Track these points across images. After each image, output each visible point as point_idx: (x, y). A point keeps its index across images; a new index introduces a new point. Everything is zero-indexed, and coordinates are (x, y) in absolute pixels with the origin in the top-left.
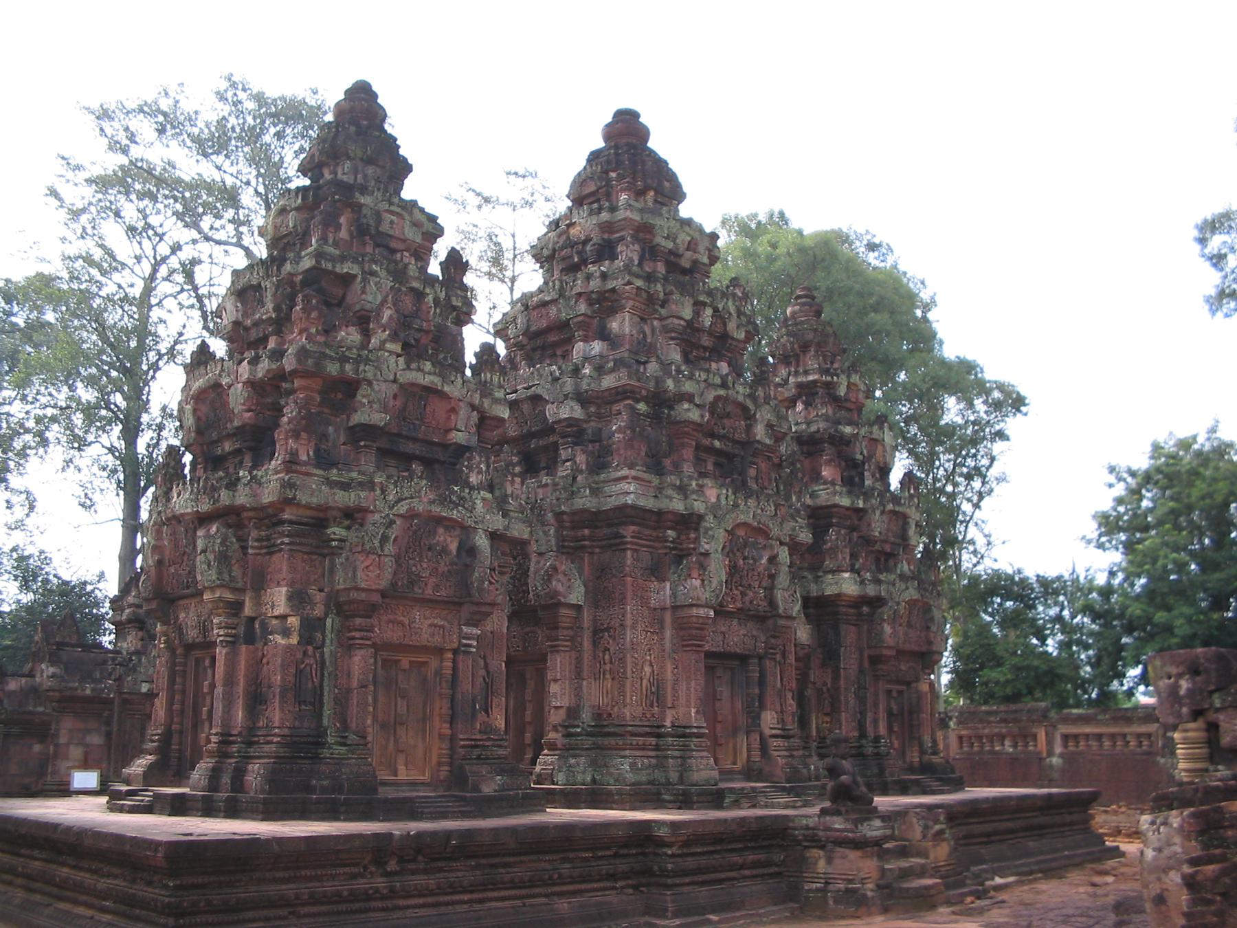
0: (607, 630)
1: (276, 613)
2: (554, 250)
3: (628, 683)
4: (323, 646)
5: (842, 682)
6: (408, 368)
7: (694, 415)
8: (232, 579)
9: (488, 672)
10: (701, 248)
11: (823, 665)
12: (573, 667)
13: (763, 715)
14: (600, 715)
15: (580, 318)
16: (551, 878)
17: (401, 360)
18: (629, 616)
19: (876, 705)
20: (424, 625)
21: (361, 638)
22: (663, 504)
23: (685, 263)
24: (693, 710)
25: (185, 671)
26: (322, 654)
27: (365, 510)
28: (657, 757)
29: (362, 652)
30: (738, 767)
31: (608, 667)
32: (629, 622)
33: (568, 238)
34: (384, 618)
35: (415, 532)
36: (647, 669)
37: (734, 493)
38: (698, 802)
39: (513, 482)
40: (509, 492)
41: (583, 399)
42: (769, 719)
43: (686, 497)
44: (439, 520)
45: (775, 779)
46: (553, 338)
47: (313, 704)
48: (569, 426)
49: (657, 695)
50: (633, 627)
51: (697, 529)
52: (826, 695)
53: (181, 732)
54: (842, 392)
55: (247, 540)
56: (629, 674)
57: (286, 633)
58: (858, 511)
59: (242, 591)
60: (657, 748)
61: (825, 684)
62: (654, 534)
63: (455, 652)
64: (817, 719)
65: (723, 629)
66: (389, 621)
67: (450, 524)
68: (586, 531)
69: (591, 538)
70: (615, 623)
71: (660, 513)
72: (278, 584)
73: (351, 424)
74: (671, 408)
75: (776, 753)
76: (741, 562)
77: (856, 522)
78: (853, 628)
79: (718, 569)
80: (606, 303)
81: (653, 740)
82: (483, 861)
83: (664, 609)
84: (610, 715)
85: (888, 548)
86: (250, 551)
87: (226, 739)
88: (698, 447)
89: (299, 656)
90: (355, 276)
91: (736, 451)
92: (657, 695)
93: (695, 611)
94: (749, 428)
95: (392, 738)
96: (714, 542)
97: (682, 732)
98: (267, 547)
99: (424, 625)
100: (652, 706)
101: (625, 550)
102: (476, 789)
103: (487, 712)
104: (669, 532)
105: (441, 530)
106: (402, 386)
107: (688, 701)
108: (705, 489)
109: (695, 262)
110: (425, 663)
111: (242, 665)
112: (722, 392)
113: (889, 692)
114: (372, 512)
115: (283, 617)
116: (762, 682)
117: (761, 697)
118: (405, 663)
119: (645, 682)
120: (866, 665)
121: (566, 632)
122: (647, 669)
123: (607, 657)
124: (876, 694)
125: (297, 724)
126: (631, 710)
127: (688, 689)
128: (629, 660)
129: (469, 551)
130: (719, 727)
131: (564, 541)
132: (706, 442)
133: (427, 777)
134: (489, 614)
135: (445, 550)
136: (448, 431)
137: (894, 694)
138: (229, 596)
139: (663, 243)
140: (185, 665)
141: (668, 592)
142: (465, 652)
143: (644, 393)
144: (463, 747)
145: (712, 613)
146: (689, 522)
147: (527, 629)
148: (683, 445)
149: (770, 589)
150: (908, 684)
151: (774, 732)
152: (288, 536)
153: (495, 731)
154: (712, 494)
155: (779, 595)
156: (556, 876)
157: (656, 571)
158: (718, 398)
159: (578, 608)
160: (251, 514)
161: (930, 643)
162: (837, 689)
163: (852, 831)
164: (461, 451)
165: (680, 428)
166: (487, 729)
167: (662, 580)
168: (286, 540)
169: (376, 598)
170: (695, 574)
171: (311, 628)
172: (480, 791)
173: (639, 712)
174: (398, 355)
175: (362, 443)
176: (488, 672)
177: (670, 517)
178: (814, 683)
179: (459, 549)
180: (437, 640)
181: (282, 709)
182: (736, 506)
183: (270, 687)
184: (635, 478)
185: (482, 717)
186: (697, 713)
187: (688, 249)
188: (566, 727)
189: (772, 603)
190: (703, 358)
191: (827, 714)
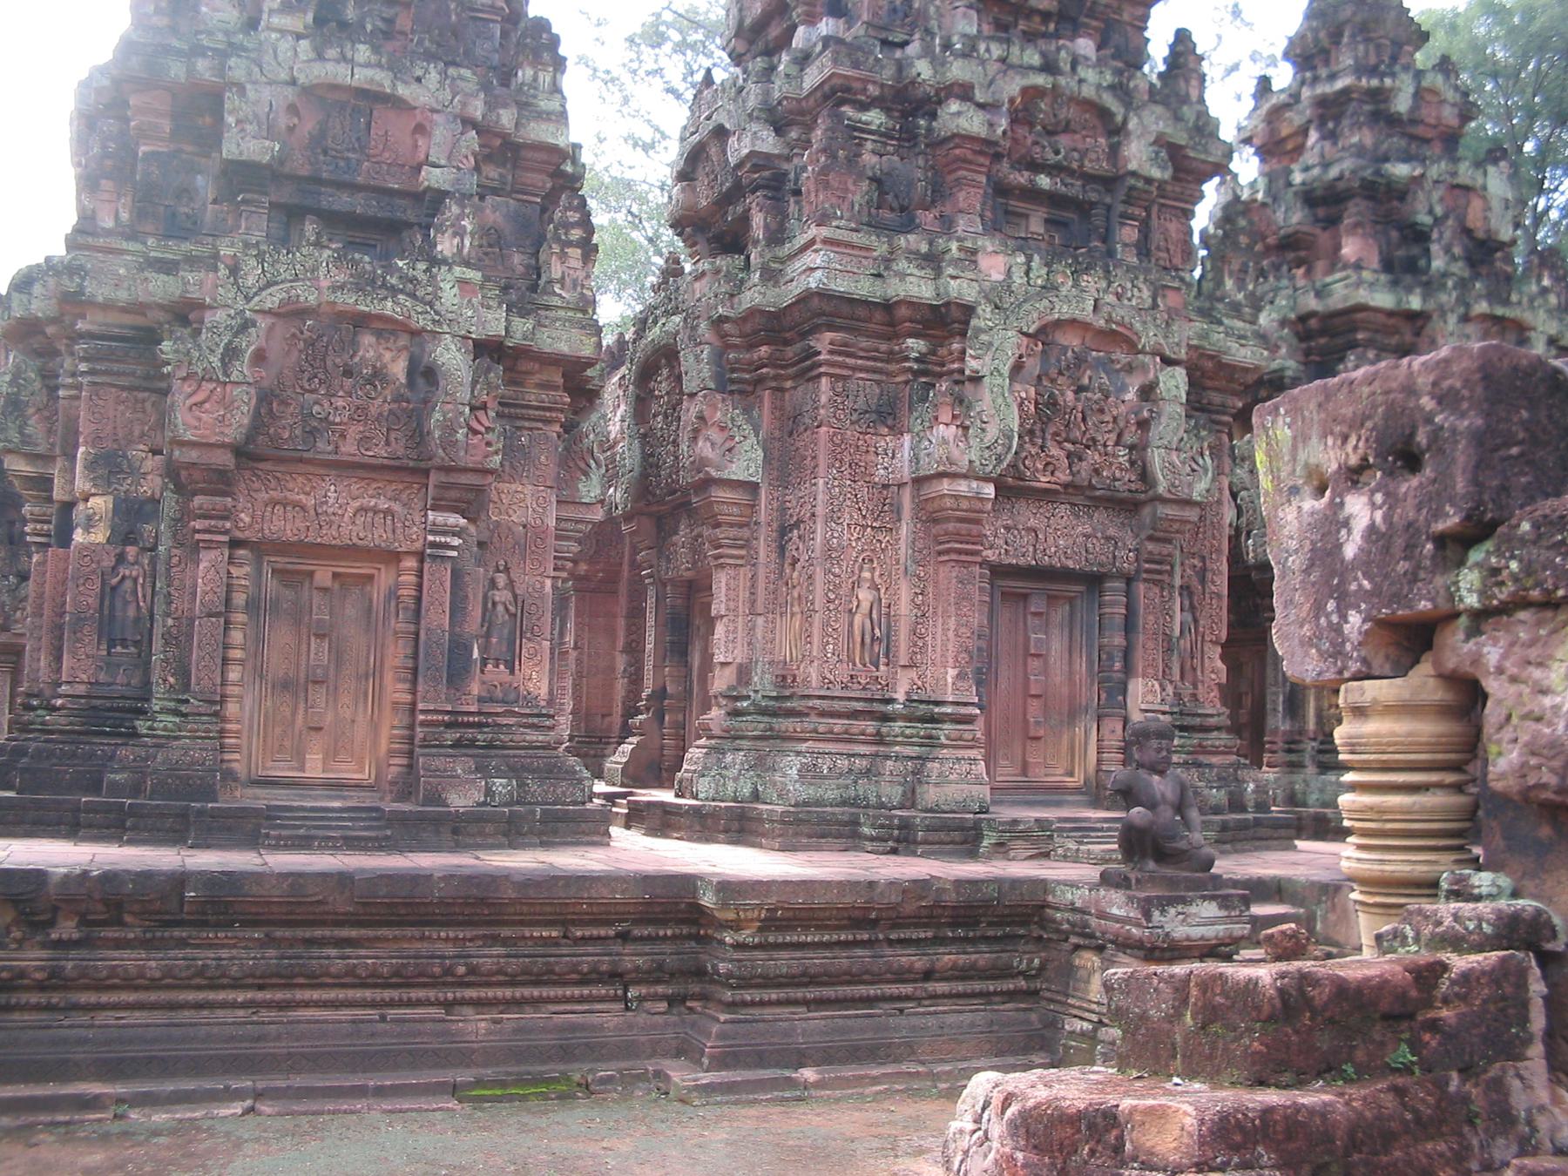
3: (817, 618)
4: (154, 548)
6: (320, 57)
7: (972, 122)
8: (26, 439)
9: (515, 596)
13: (1131, 687)
16: (449, 971)
17: (304, 44)
18: (820, 497)
20: (343, 509)
22: (896, 289)
24: (952, 673)
26: (153, 562)
27: (201, 306)
28: (876, 755)
29: (212, 554)
30: (1077, 779)
32: (820, 510)
34: (263, 496)
35: (311, 343)
36: (865, 595)
38: (926, 842)
39: (563, 257)
44: (361, 321)
47: (136, 643)
48: (756, 168)
49: (879, 643)
50: (833, 517)
51: (963, 334)
58: (1411, 316)
59: (48, 458)
62: (884, 347)
63: (421, 556)
64: (1318, 699)
65: (1032, 523)
67: (387, 328)
69: (771, 362)
70: (805, 512)
71: (888, 307)
74: (933, 116)
76: (1070, 395)
77: (1408, 338)
79: (1000, 409)
81: (870, 726)
82: (279, 933)
83: (901, 485)
88: (1001, 190)
91: (1093, 197)
92: (879, 643)
93: (945, 486)
94: (1114, 152)
95: (302, 706)
96: (993, 352)
97: (925, 713)
99: (343, 509)
102: (435, 798)
104: (910, 342)
105: (367, 339)
108: (980, 257)
110: (371, 577)
112: (1040, 80)
114: (210, 307)
116: (1129, 625)
117: (1127, 654)
118: (323, 576)
119: (858, 619)
125: (102, 677)
129: (425, 374)
130: (1034, 705)
132: (1022, 178)
135: (379, 375)
142: (434, 557)
143: (873, 90)
144: (423, 724)
146: (946, 322)
153: (530, 700)
154: (994, 265)
155: (1156, 459)
156: (461, 970)
157: (887, 416)
159: (754, 487)
163: (1138, 925)
164: (435, 200)
166: (512, 697)
167: (897, 431)
169: (225, 459)
170: (945, 416)
171: (131, 518)
174: (299, 37)
179: (411, 372)
180: (379, 536)
182: (1050, 287)
184: (826, 241)
186: (960, 676)
189: (1145, 476)
190: (1044, 35)
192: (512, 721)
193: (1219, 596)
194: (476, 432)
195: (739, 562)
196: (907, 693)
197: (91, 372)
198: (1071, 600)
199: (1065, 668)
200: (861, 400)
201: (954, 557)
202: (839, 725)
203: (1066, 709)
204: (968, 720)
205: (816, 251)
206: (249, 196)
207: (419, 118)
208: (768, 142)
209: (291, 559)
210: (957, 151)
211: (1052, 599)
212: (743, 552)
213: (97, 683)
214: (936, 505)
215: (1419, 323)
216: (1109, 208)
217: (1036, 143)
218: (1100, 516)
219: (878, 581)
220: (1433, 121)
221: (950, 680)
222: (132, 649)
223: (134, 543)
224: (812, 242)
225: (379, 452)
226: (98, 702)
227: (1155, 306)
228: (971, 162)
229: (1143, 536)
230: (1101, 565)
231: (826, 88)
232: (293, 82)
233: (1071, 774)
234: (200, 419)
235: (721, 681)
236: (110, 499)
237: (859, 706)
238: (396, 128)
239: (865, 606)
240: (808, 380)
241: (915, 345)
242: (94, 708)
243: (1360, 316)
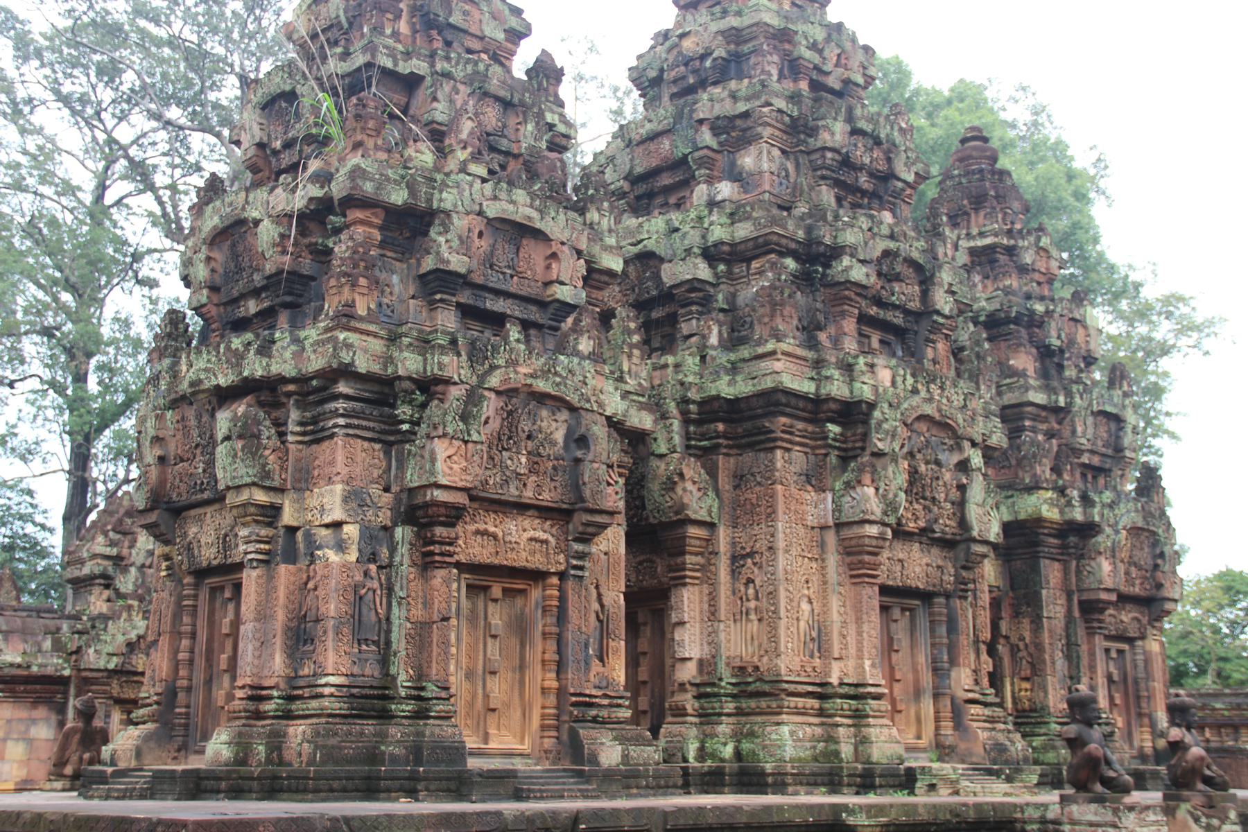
0: (751, 555)
1: (328, 519)
2: (662, 70)
3: (783, 623)
5: (1046, 634)
7: (859, 274)
9: (602, 606)
10: (854, 64)
11: (1016, 615)
12: (706, 606)
13: (953, 674)
14: (742, 669)
15: (701, 153)
18: (781, 536)
19: (1092, 668)
21: (442, 554)
23: (833, 82)
24: (867, 663)
25: (195, 606)
28: (822, 724)
30: (924, 742)
31: (752, 604)
32: (781, 544)
33: (680, 53)
34: (472, 528)
37: (913, 375)
39: (630, 356)
40: (626, 368)
41: (710, 254)
42: (962, 680)
43: (852, 380)
45: (974, 759)
46: (666, 180)
47: (376, 643)
49: (819, 642)
51: (866, 422)
52: (1023, 654)
53: (189, 689)
54: (1028, 258)
55: (285, 424)
56: (783, 613)
57: (341, 547)
58: (1056, 410)
60: (821, 713)
61: (1022, 639)
64: (1012, 684)
65: (901, 556)
66: (478, 532)
67: (559, 403)
68: (721, 427)
69: (725, 436)
70: (761, 545)
72: (330, 481)
73: (422, 271)
74: (827, 266)
75: (975, 724)
77: (1056, 426)
78: (1056, 565)
80: (736, 131)
81: (815, 703)
83: (823, 528)
84: (757, 668)
85: (1096, 461)
86: (290, 438)
87: (257, 695)
88: (863, 319)
89: (359, 577)
90: (422, 78)
92: (819, 642)
94: (925, 295)
98: (312, 432)
100: (812, 656)
101: (773, 449)
103: (602, 660)
106: (490, 221)
107: (860, 650)
108: (876, 369)
109: (847, 82)
110: (523, 591)
111: (282, 593)
112: (892, 245)
113: (1107, 651)
114: (455, 383)
115: (337, 525)
119: (802, 624)
120: (1077, 614)
121: (694, 559)
122: (805, 606)
123: (751, 591)
124: (1092, 654)
125: (356, 670)
126: (790, 662)
127: (860, 633)
128: (782, 594)
130: (897, 686)
131: (689, 439)
132: (873, 311)
133: (526, 747)
134: (604, 527)
136: (547, 284)
137: (1114, 655)
138: (261, 497)
139: (808, 54)
140: (196, 597)
141: (830, 506)
145: (889, 532)
146: (854, 414)
147: (642, 558)
148: (843, 314)
149: (961, 504)
150: (1130, 641)
151: (971, 695)
152: (342, 415)
155: (973, 512)
158: (886, 253)
159: (711, 526)
160: (291, 387)
161: (1159, 586)
162: (1039, 647)
165: (843, 291)
168: (341, 421)
169: (461, 499)
172: (598, 764)
173: (796, 664)
174: (484, 181)
175: (438, 297)
176: (602, 606)
177: (833, 406)
178: (1007, 637)
179: (567, 437)
181: (337, 651)
182: (915, 391)
183: (317, 621)
185: (596, 666)
186: (873, 665)
187: (837, 65)
188: (697, 685)
189: (963, 524)
191: (1027, 679)
192: (606, 702)
193: (984, 608)
194: (609, 484)
195: (697, 582)
196: (841, 679)
197: (347, 426)
198: (911, 610)
199: (909, 660)
200: (798, 467)
201: (867, 580)
202: (800, 702)
203: (911, 690)
204: (877, 697)
205: (779, 360)
206: (445, 297)
207: (554, 249)
208: (703, 271)
209: (482, 577)
210: (847, 292)
211: (903, 610)
212: (698, 574)
213: (352, 675)
214: (853, 542)
215: (1062, 415)
216: (916, 333)
217: (882, 288)
218: (935, 551)
219: (812, 596)
220: (1043, 270)
221: (867, 669)
222: (374, 648)
223: (375, 561)
224: (773, 353)
225: (547, 497)
226: (355, 691)
227: (965, 406)
228: (851, 300)
229: (958, 566)
230: (934, 586)
231: (761, 240)
232: (480, 213)
233: (919, 737)
234: (451, 468)
235: (687, 673)
236: (358, 526)
237: (810, 688)
238: (534, 254)
239: (806, 613)
240: (760, 450)
241: (834, 429)
242: (352, 696)
243: (1029, 409)
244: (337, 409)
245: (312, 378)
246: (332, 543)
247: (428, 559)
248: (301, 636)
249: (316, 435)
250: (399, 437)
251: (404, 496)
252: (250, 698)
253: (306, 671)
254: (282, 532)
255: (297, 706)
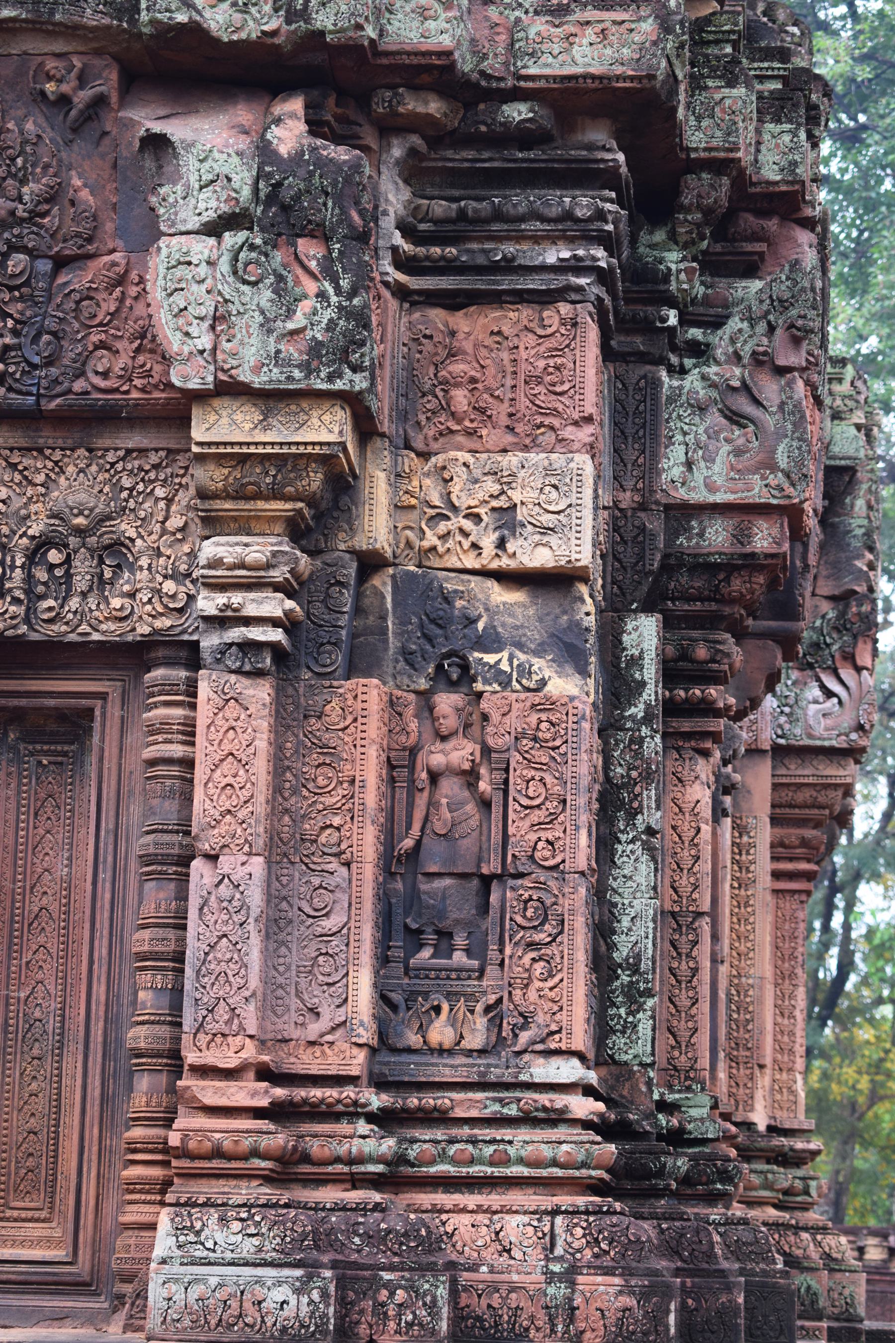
244: (601, 215)
245: (516, 95)
246: (535, 634)
247: (686, 726)
248: (433, 914)
249: (457, 270)
250: (639, 343)
251: (655, 524)
252: (277, 1113)
253: (440, 1032)
254: (352, 570)
255: (424, 1141)
